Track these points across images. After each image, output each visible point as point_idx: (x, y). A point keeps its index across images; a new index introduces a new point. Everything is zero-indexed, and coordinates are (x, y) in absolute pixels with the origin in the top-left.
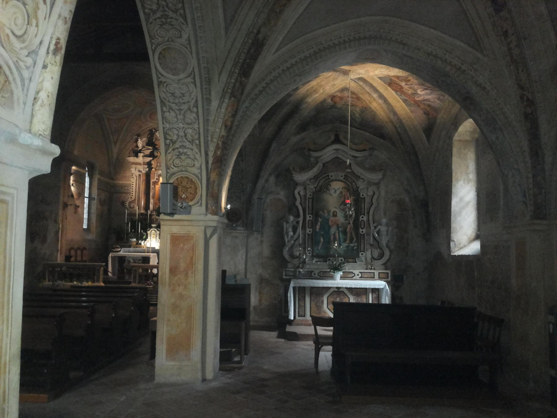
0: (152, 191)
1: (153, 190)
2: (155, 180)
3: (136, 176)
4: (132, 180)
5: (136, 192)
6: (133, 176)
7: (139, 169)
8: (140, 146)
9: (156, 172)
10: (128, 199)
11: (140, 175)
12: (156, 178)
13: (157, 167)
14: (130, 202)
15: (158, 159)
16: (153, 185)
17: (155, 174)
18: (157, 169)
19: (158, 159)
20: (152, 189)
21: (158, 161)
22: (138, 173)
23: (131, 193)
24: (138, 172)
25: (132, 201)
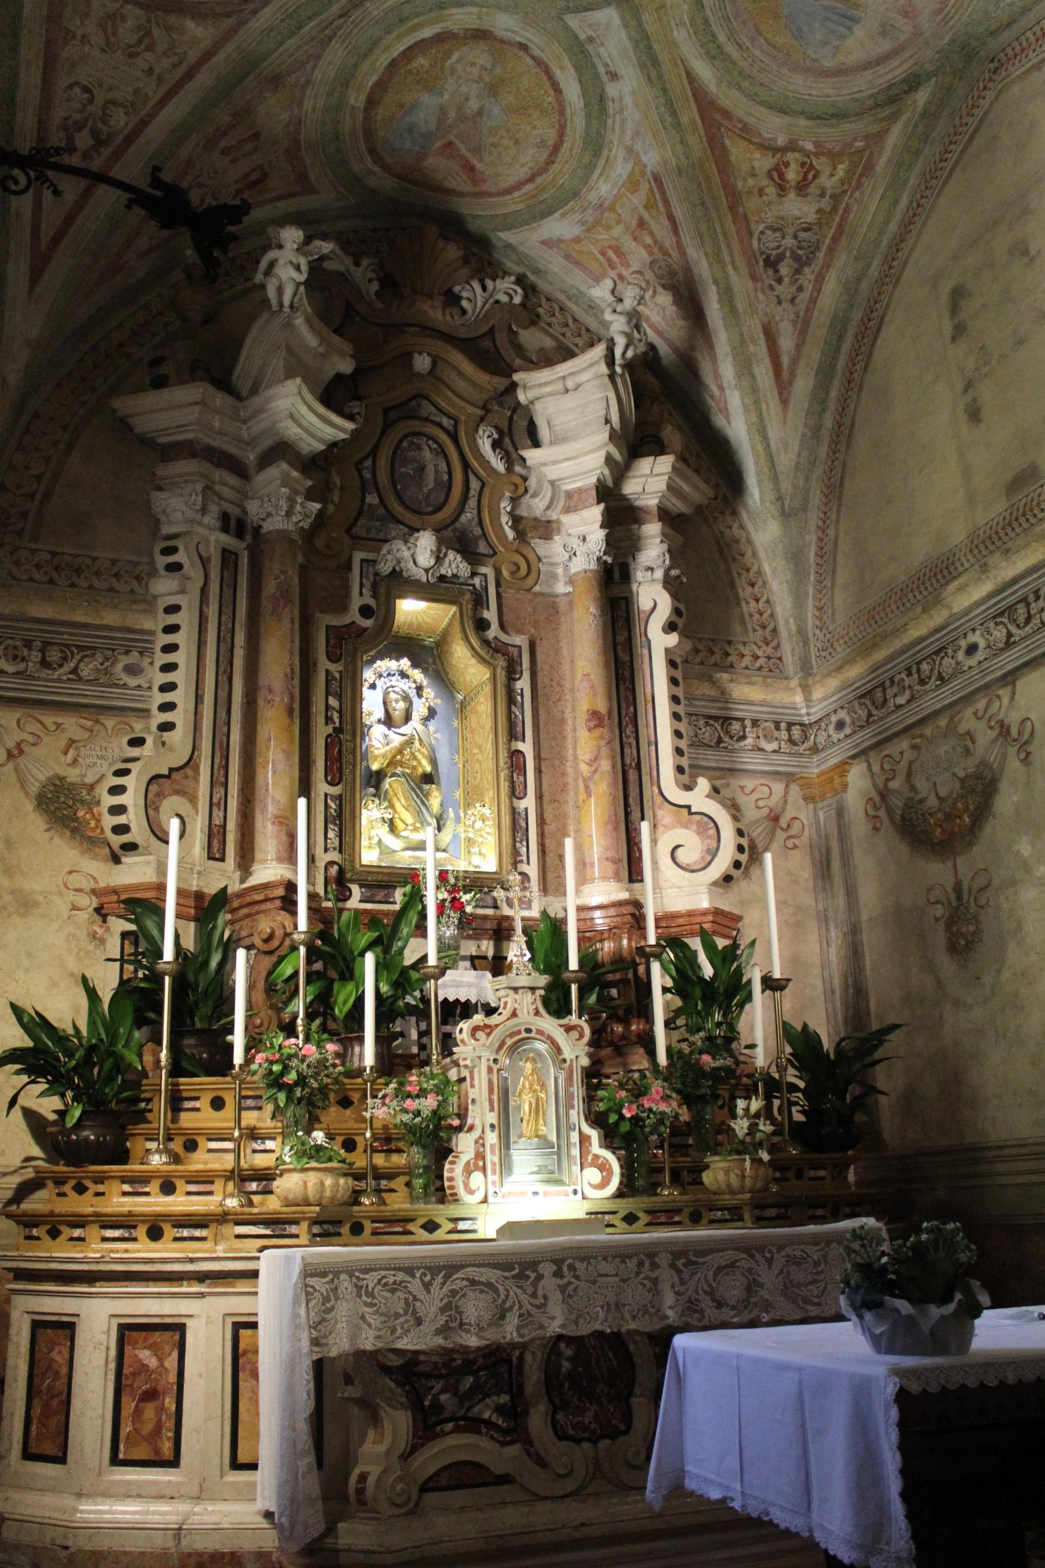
0: (328, 707)
1: (333, 702)
2: (353, 615)
3: (204, 562)
4: (164, 586)
5: (199, 698)
6: (180, 557)
7: (229, 508)
8: (280, 290)
9: (358, 556)
10: (135, 752)
11: (228, 558)
12: (356, 602)
13: (362, 522)
14: (156, 777)
15: (368, 463)
16: (333, 658)
17: (349, 566)
18: (359, 530)
19: (368, 463)
20: (328, 693)
21: (367, 475)
22: (217, 540)
23: (145, 713)
24: (218, 524)
25: (171, 770)
